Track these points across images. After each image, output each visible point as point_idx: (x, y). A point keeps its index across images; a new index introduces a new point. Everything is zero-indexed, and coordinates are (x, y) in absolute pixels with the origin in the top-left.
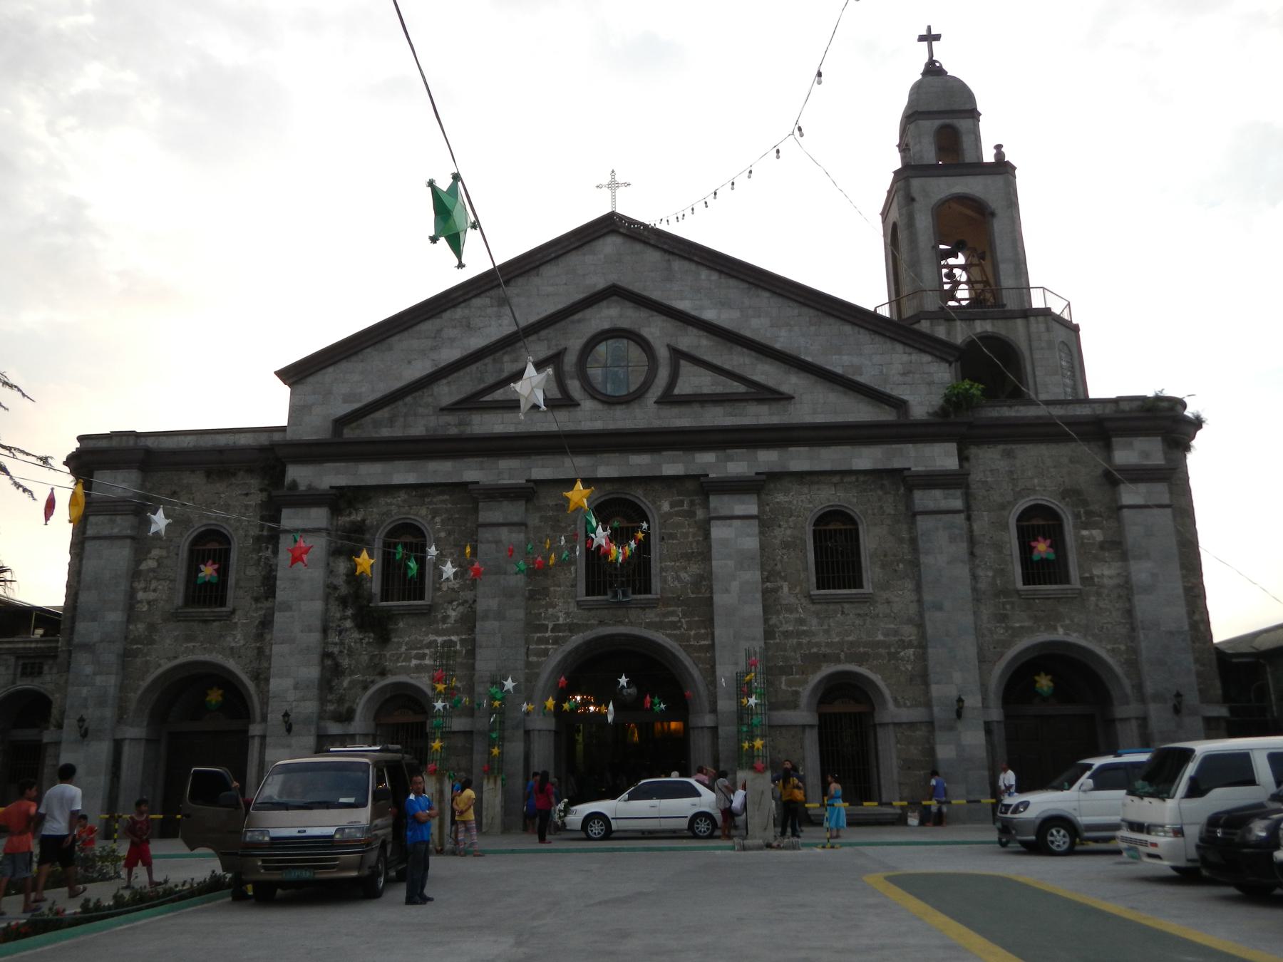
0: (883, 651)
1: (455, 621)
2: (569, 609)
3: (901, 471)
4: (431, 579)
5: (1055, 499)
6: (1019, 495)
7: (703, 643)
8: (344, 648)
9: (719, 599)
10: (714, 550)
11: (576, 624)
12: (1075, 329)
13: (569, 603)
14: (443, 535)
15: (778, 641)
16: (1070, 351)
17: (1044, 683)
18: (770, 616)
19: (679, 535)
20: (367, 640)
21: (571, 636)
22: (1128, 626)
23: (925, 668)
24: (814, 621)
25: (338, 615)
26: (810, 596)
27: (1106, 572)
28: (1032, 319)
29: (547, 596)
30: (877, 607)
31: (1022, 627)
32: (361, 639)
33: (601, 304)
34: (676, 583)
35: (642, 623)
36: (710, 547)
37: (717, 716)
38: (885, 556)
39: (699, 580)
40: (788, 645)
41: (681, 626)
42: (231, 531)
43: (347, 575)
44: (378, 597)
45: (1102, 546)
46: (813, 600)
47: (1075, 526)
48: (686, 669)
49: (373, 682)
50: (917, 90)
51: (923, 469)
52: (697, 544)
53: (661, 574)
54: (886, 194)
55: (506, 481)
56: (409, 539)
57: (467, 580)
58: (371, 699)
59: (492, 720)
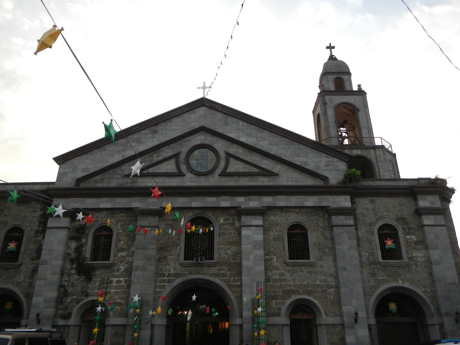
0: (319, 289)
1: (123, 271)
2: (175, 266)
3: (326, 207)
4: (114, 251)
5: (394, 222)
6: (378, 220)
7: (237, 283)
8: (70, 283)
9: (244, 263)
10: (242, 240)
11: (179, 273)
12: (394, 155)
13: (176, 264)
14: (121, 231)
15: (271, 283)
16: (392, 163)
17: (393, 307)
18: (267, 272)
19: (227, 234)
20: (81, 279)
22: (430, 280)
23: (339, 297)
24: (288, 275)
25: (69, 267)
26: (286, 263)
27: (419, 255)
28: (377, 150)
29: (166, 260)
30: (317, 268)
31: (382, 279)
32: (79, 279)
33: (197, 134)
34: (225, 255)
35: (209, 274)
36: (241, 239)
37: (243, 319)
38: (320, 245)
39: (235, 254)
40: (276, 285)
41: (227, 276)
42: (25, 227)
43: (75, 249)
44: (89, 259)
45: (416, 243)
46: (287, 264)
47: (404, 234)
48: (229, 296)
49: (82, 300)
50: (326, 65)
51: (336, 206)
52: (235, 238)
53: (218, 251)
54: (314, 104)
55: (151, 207)
56: (105, 233)
57: (130, 252)
58: (80, 308)
59: (135, 319)
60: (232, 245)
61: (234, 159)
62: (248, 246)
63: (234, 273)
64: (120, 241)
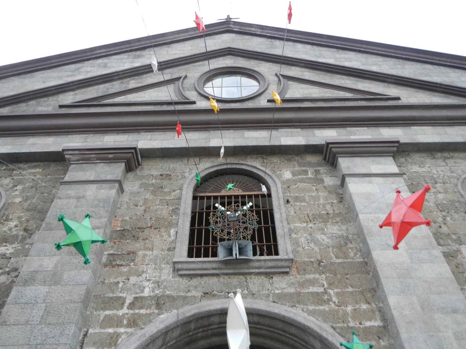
2: (160, 277)
7: (368, 324)
11: (168, 296)
13: (161, 269)
21: (159, 314)
34: (312, 245)
35: (268, 296)
41: (330, 300)
52: (332, 206)
53: (290, 235)
60: (325, 222)
61: (296, 83)
62: (376, 215)
63: (352, 292)
64: (7, 220)
